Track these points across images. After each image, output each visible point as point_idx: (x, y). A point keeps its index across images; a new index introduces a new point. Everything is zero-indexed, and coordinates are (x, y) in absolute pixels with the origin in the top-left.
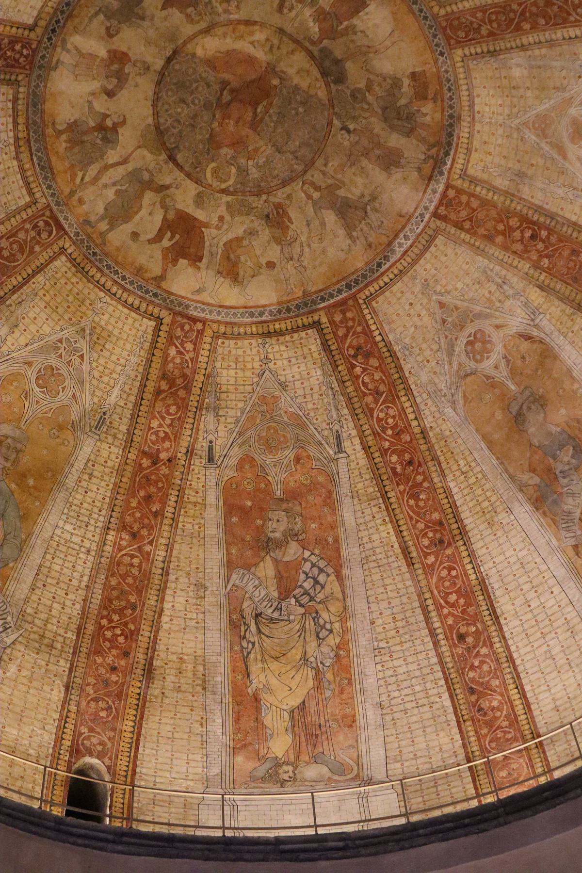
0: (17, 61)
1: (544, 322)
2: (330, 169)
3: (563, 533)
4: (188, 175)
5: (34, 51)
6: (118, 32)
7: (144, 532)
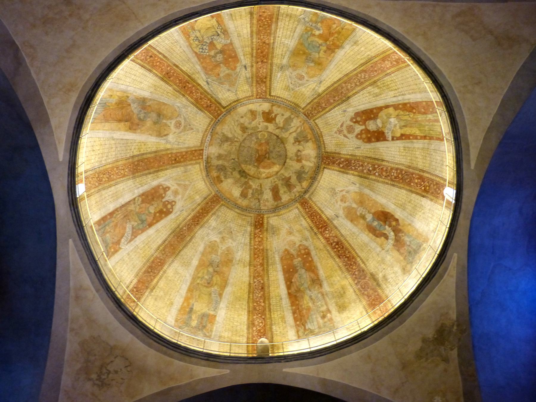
0: (327, 159)
1: (163, 142)
2: (234, 147)
3: (133, 98)
4: (272, 133)
5: (322, 161)
6: (301, 168)
7: (261, 44)
